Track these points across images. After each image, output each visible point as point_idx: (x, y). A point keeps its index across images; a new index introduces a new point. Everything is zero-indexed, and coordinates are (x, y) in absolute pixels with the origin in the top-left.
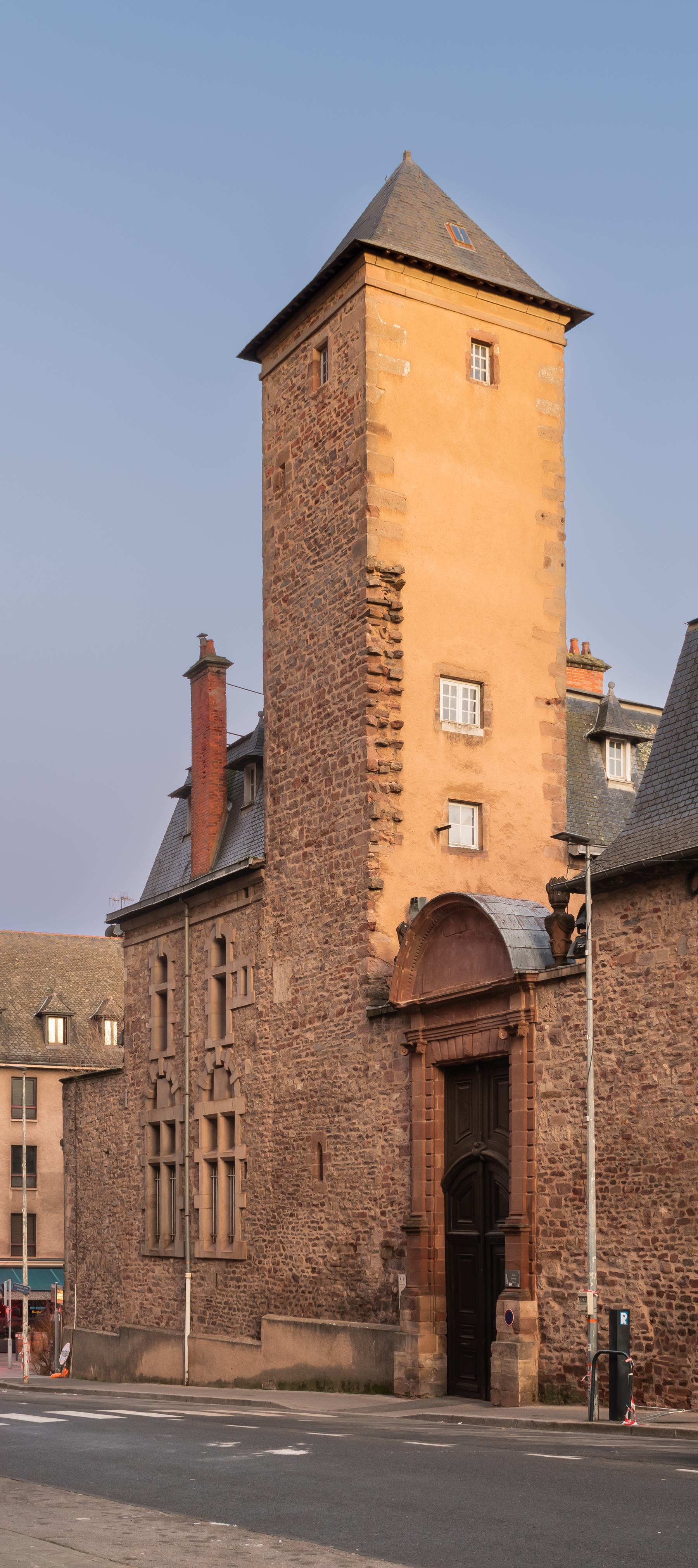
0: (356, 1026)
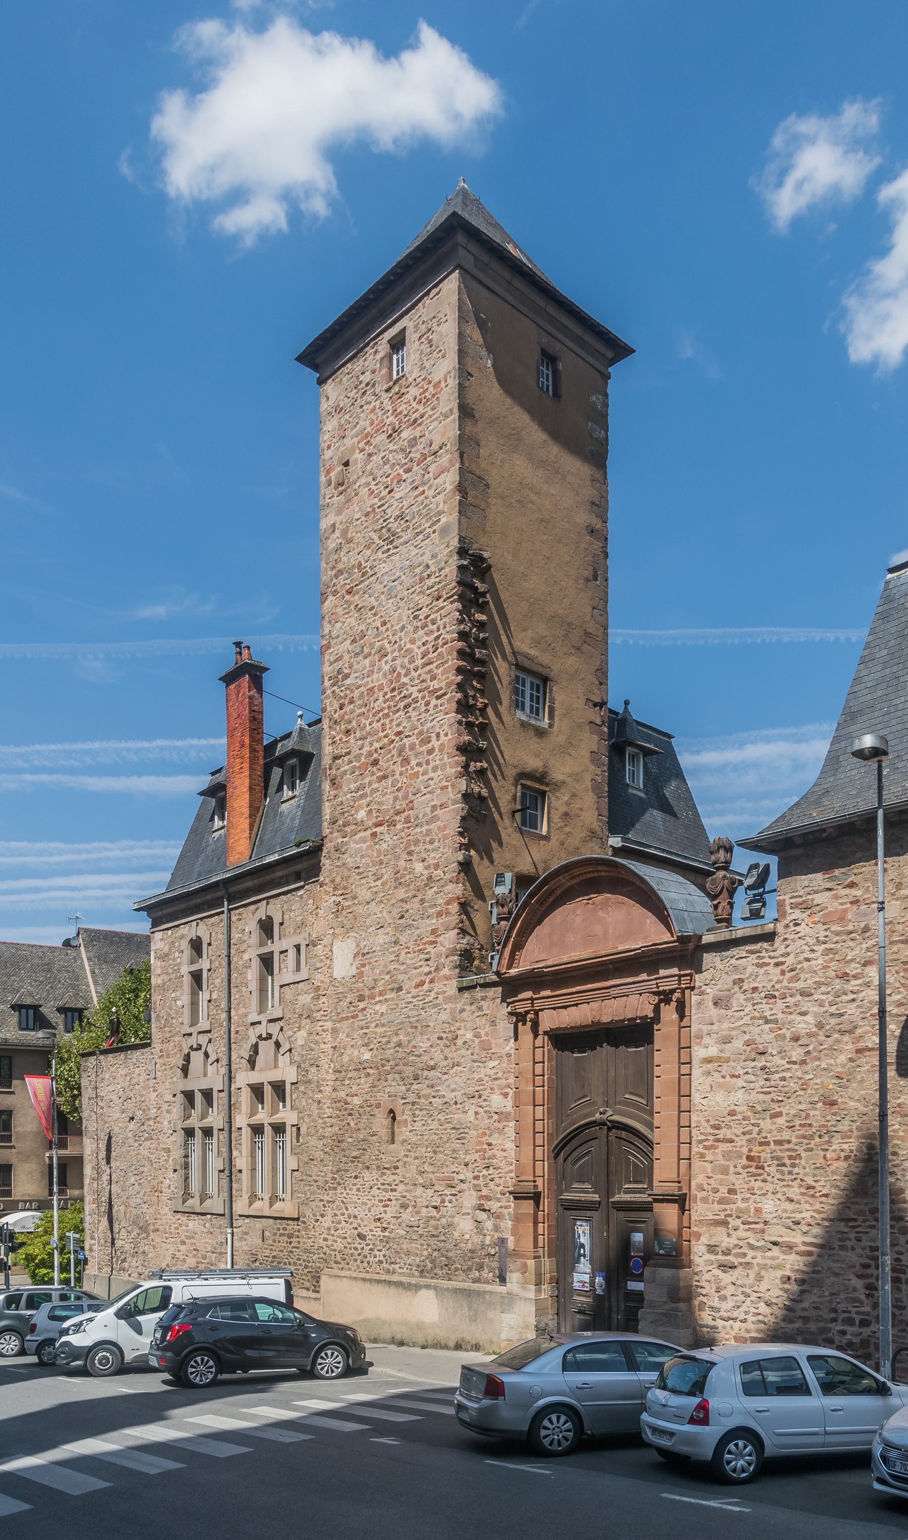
0: (440, 997)
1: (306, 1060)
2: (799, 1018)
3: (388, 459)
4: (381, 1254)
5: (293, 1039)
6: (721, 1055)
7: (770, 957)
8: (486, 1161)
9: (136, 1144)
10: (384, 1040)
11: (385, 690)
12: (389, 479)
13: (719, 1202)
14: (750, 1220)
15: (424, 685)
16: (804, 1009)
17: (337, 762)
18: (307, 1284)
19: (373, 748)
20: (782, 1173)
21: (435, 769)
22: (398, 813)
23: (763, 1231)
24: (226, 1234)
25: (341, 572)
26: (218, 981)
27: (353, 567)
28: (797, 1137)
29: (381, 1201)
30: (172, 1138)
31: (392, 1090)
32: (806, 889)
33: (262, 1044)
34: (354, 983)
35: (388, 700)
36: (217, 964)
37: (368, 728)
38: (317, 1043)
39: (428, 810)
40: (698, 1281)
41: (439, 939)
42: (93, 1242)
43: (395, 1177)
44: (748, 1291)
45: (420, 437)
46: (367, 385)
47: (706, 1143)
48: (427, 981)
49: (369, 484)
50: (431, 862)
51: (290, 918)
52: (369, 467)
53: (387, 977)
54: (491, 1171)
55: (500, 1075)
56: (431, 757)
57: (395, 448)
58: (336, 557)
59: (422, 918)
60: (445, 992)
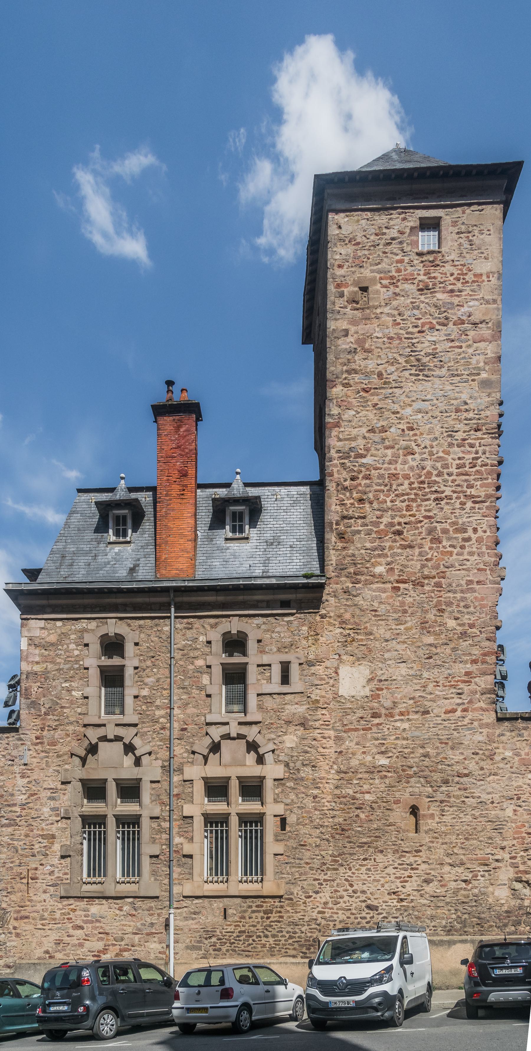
34: (367, 702)
35: (415, 488)
43: (417, 859)
50: (467, 621)
57: (427, 301)
59: (455, 662)
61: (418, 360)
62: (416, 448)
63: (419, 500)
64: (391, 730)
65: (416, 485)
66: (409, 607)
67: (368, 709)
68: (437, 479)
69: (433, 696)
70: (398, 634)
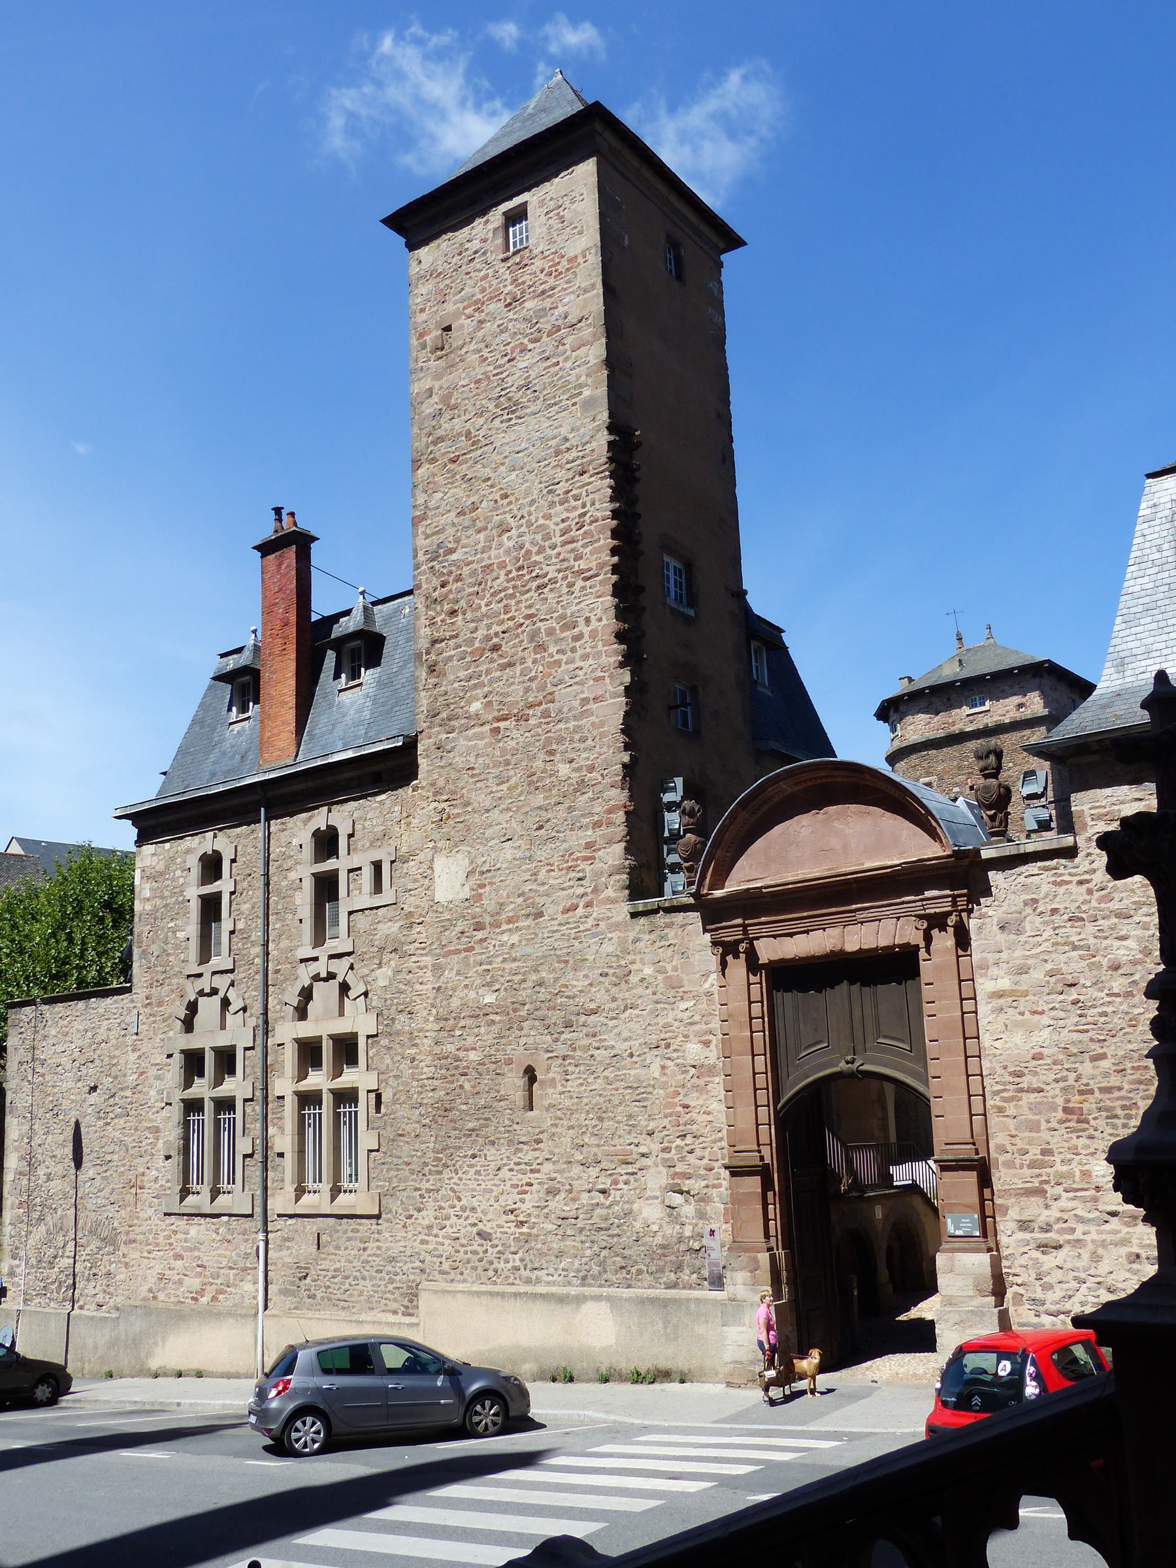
0: (603, 924)
1: (391, 1005)
2: (1117, 943)
3: (507, 328)
4: (517, 1257)
5: (369, 979)
6: (1015, 988)
7: (1070, 874)
8: (681, 1128)
9: (101, 1123)
10: (517, 978)
11: (509, 568)
12: (508, 348)
13: (1031, 1166)
14: (1074, 1186)
15: (565, 564)
16: (1122, 933)
17: (438, 646)
18: (393, 1306)
19: (492, 631)
20: (1114, 1126)
21: (585, 657)
22: (531, 706)
23: (1095, 1200)
24: (254, 1241)
25: (441, 439)
26: (245, 907)
27: (459, 434)
28: (1131, 1083)
29: (515, 1186)
30: (164, 1113)
31: (531, 1040)
32: (1109, 799)
33: (318, 987)
34: (468, 908)
35: (513, 579)
36: (245, 884)
37: (484, 609)
38: (408, 983)
39: (576, 703)
40: (1009, 1267)
41: (597, 855)
42: (17, 1262)
43: (537, 1154)
44: (1083, 1275)
45: (551, 309)
46: (476, 252)
47: (1005, 1094)
48: (581, 905)
49: (480, 351)
51: (364, 828)
52: (480, 334)
53: (520, 900)
54: (689, 1140)
55: (697, 1018)
56: (578, 644)
57: (515, 317)
58: (434, 423)
59: (571, 830)
60: (608, 918)
61: (510, 399)
62: (511, 521)
63: (518, 594)
64: (497, 948)
65: (514, 574)
66: (513, 755)
67: (470, 918)
68: (539, 558)
69: (547, 887)
70: (500, 798)
